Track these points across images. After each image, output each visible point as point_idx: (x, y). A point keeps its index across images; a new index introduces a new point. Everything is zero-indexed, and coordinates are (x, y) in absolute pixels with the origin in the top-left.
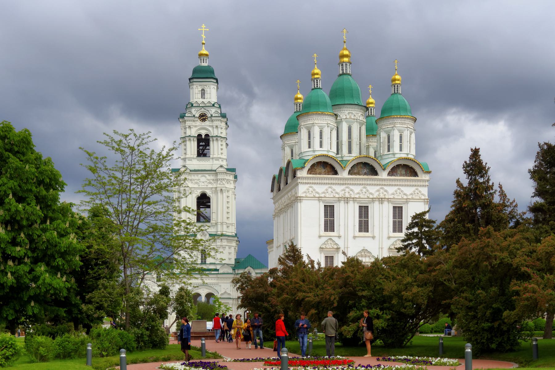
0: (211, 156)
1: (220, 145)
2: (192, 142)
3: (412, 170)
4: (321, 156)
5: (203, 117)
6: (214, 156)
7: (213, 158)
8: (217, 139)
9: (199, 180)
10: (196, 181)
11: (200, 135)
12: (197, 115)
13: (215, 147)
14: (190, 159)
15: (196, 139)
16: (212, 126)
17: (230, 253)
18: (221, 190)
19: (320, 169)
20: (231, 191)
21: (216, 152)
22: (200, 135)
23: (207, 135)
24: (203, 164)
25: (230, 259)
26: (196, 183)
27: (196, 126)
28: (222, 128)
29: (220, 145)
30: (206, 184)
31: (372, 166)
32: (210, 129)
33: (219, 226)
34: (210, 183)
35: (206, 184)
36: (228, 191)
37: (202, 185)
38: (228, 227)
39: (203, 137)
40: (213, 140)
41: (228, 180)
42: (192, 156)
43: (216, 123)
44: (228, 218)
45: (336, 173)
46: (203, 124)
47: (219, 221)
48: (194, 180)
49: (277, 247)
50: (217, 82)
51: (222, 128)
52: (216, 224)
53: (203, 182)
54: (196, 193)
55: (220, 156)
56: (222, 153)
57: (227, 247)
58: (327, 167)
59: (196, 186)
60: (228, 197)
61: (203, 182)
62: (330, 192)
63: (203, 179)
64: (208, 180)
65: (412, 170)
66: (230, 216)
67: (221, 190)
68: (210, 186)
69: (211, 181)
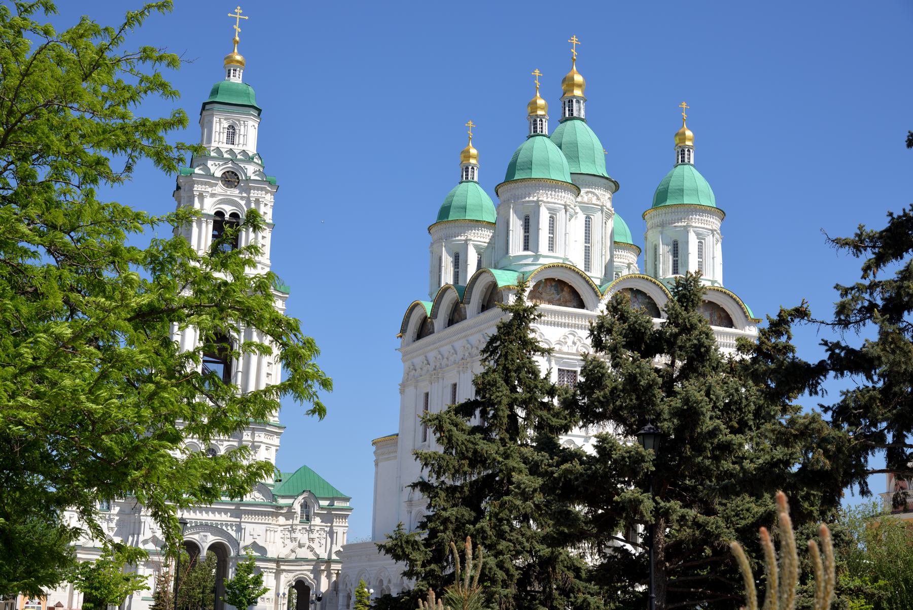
3: (723, 315)
4: (554, 266)
5: (231, 179)
11: (220, 214)
12: (218, 174)
19: (550, 291)
22: (220, 214)
27: (213, 195)
28: (266, 205)
31: (649, 298)
32: (243, 203)
39: (227, 217)
45: (582, 305)
46: (228, 193)
51: (266, 205)
58: (562, 290)
62: (570, 343)
65: (723, 315)
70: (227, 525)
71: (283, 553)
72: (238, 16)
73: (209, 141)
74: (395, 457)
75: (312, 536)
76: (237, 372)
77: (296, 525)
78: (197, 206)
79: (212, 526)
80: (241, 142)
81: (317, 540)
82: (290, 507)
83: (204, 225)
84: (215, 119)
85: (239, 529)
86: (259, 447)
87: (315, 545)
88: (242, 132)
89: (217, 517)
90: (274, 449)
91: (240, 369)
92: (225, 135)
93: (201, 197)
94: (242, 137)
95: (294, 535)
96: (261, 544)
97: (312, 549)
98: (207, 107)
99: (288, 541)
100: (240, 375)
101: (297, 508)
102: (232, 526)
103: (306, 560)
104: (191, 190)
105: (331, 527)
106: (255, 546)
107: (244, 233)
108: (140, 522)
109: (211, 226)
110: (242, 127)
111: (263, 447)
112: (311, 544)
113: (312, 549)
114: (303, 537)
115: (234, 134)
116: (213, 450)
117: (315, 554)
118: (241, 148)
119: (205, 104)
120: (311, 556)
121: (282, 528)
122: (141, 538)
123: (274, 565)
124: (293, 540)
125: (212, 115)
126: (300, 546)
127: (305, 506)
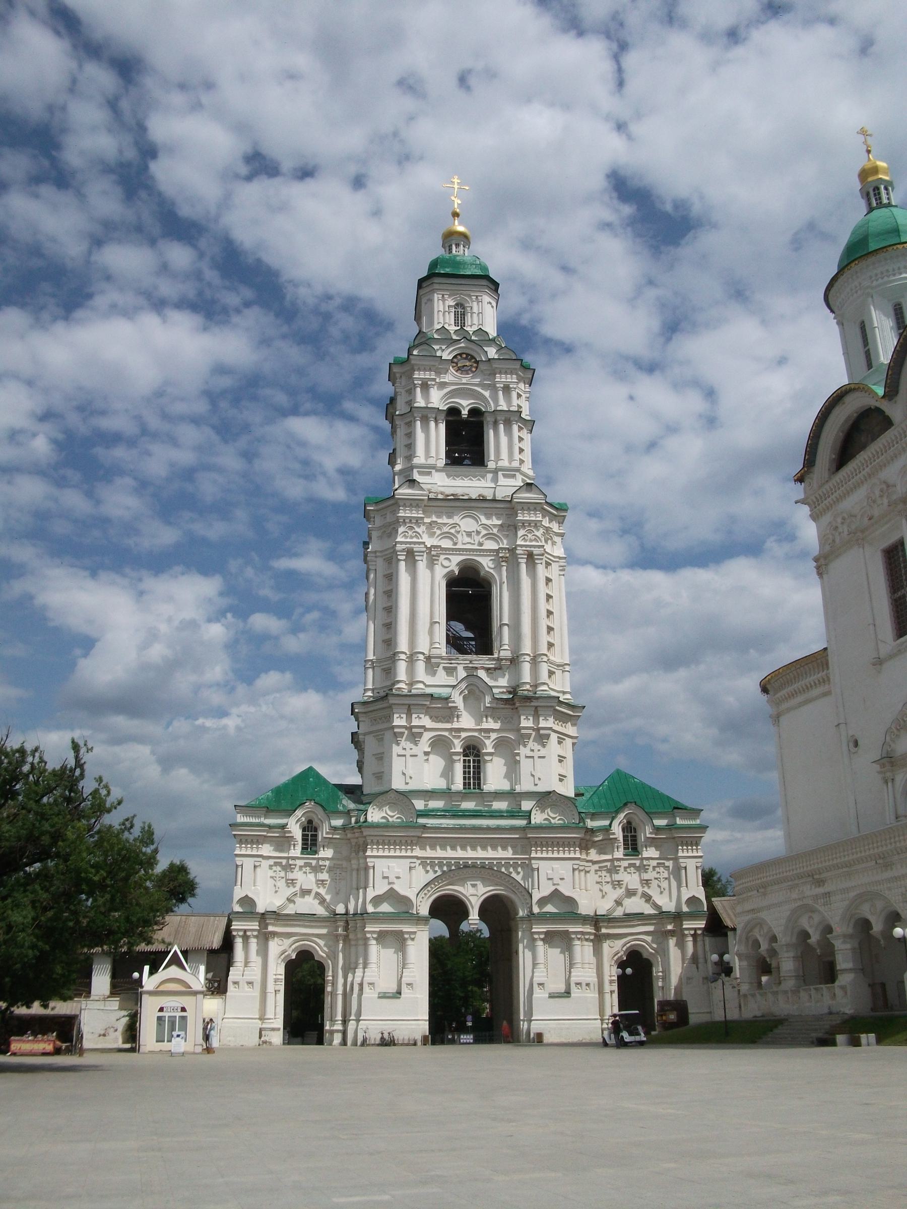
0: (491, 465)
1: (516, 439)
2: (432, 424)
5: (468, 361)
6: (500, 464)
7: (495, 472)
8: (508, 423)
9: (455, 525)
10: (445, 529)
11: (453, 412)
13: (500, 445)
14: (427, 470)
15: (443, 416)
16: (493, 388)
17: (561, 759)
18: (530, 556)
20: (555, 566)
21: (504, 454)
22: (453, 412)
23: (474, 412)
24: (470, 484)
25: (562, 778)
26: (447, 536)
27: (442, 385)
29: (516, 439)
30: (477, 539)
32: (487, 394)
33: (526, 668)
34: (490, 537)
35: (477, 539)
36: (548, 564)
37: (463, 541)
38: (551, 673)
39: (465, 412)
40: (496, 423)
41: (548, 529)
42: (431, 461)
43: (501, 379)
44: (550, 645)
46: (464, 381)
47: (527, 648)
48: (440, 526)
49: (879, 662)
50: (496, 290)
52: (515, 661)
53: (469, 534)
54: (446, 563)
55: (516, 464)
56: (522, 462)
57: (554, 737)
59: (446, 544)
60: (548, 580)
61: (469, 534)
63: (467, 524)
64: (485, 526)
66: (555, 638)
67: (530, 556)
68: (491, 545)
69: (495, 531)
70: (507, 865)
71: (604, 907)
72: (456, 186)
73: (431, 322)
74: (827, 694)
75: (646, 876)
76: (502, 625)
77: (619, 860)
78: (420, 402)
79: (483, 867)
80: (475, 321)
81: (654, 883)
82: (607, 830)
83: (432, 424)
84: (436, 297)
85: (529, 871)
86: (548, 736)
87: (653, 892)
88: (475, 310)
89: (490, 853)
90: (569, 742)
91: (506, 621)
92: (452, 314)
93: (425, 386)
94: (475, 316)
95: (616, 877)
96: (567, 893)
97: (648, 898)
98: (424, 285)
99: (608, 888)
100: (506, 629)
101: (617, 831)
102: (515, 866)
103: (639, 917)
104: (410, 377)
105: (676, 859)
106: (556, 896)
107: (491, 432)
108: (366, 868)
109: (442, 427)
110: (475, 304)
111: (554, 737)
112: (646, 889)
113: (648, 898)
114: (632, 880)
115: (463, 315)
116: (474, 748)
117: (656, 906)
118: (475, 328)
119: (421, 282)
120: (649, 910)
121: (596, 867)
122: (371, 894)
123: (589, 929)
124: (618, 884)
125: (433, 291)
126: (630, 893)
127: (629, 829)
